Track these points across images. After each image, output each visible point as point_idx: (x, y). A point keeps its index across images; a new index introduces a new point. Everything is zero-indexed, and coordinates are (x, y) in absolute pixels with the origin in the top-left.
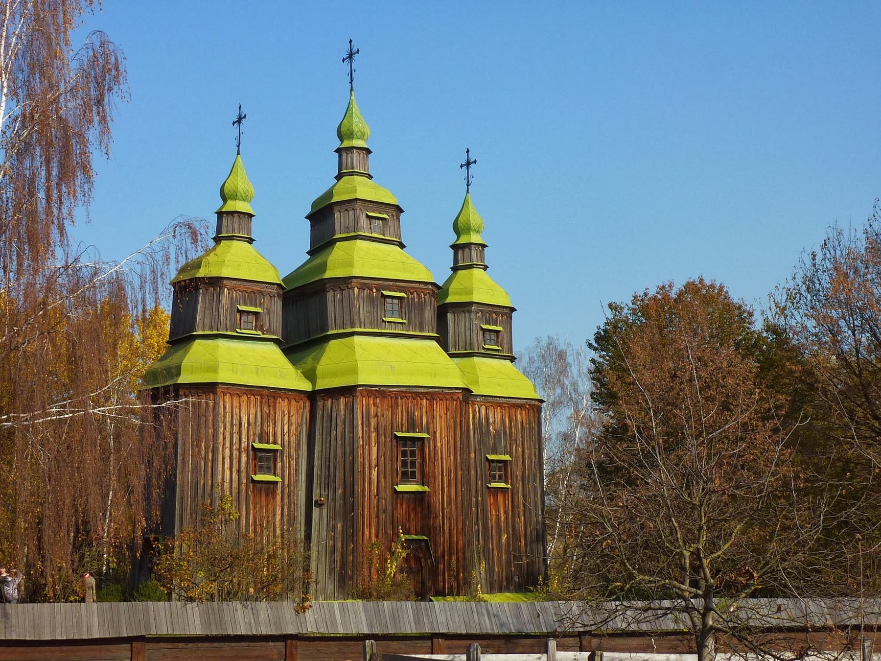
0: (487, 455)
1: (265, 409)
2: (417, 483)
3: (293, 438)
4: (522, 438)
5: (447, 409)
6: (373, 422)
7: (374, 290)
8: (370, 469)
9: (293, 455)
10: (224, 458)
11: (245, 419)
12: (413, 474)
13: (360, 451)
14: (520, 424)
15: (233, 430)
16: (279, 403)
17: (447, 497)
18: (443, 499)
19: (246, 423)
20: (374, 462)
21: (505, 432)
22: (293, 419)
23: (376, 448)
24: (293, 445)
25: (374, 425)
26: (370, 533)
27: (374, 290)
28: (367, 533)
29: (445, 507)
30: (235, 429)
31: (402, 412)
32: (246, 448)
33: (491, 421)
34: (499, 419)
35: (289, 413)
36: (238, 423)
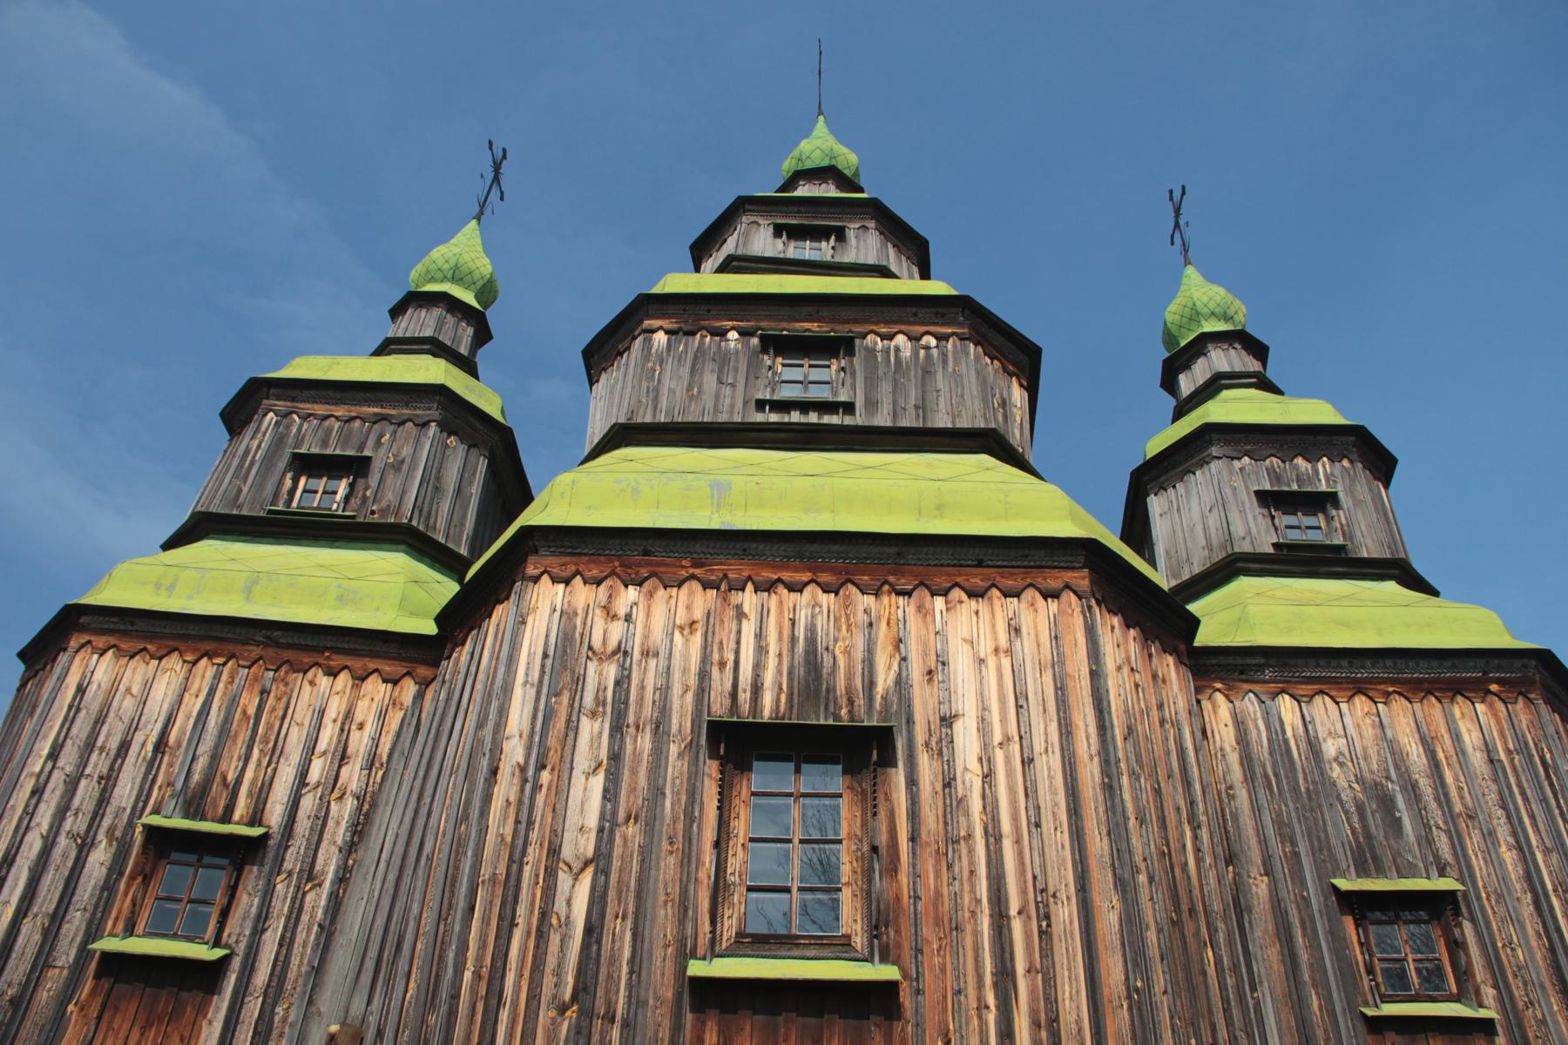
0: (1335, 881)
1: (250, 702)
2: (841, 947)
3: (343, 811)
4: (1504, 807)
5: (1015, 631)
6: (600, 676)
7: (733, 335)
8: (551, 873)
9: (323, 873)
11: (149, 733)
13: (506, 788)
14: (1477, 759)
16: (312, 683)
17: (1036, 1024)
19: (150, 747)
20: (579, 842)
21: (1411, 789)
22: (360, 743)
23: (598, 782)
24: (338, 832)
25: (600, 689)
27: (733, 335)
30: (98, 764)
31: (760, 636)
32: (118, 834)
33: (1330, 748)
34: (1369, 742)
35: (349, 715)
36: (114, 744)
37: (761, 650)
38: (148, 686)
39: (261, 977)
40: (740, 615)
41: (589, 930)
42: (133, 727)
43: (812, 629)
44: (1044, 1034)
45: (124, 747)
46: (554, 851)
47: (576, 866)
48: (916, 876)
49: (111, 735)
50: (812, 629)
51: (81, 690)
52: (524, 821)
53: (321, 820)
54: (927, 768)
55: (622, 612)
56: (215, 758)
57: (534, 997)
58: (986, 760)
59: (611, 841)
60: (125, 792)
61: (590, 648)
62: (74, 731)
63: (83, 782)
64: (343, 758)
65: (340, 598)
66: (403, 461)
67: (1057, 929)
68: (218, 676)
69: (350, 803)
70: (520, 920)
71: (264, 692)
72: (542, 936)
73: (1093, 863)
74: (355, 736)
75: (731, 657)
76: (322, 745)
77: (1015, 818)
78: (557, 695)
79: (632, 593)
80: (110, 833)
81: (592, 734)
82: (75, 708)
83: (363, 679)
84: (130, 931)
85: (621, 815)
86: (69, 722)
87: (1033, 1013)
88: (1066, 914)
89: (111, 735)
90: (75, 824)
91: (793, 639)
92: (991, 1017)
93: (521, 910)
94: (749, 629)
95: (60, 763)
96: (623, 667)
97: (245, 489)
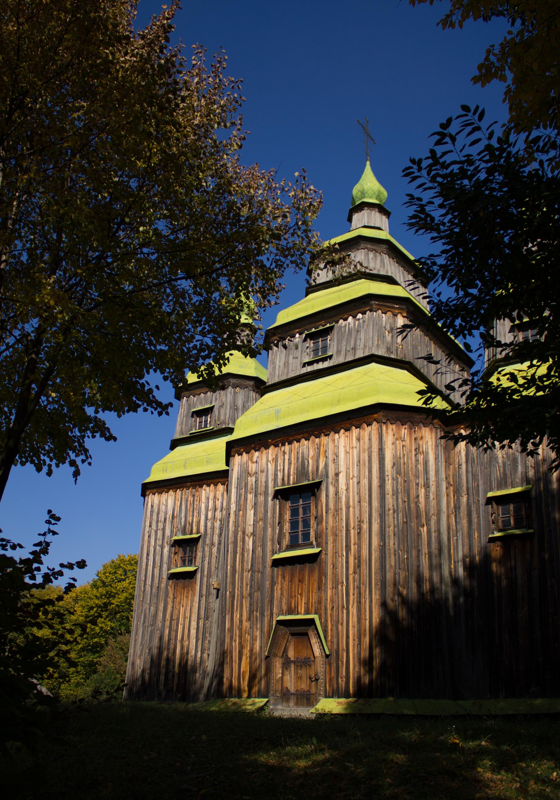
1: (190, 499)
2: (311, 545)
3: (217, 524)
10: (148, 555)
12: (306, 536)
15: (157, 526)
17: (355, 558)
18: (347, 562)
20: (250, 529)
23: (252, 512)
24: (217, 531)
26: (241, 615)
28: (237, 616)
29: (351, 570)
30: (161, 525)
31: (289, 459)
35: (215, 497)
36: (163, 519)
37: (290, 464)
38: (167, 501)
39: (206, 573)
40: (284, 453)
41: (253, 551)
42: (166, 513)
43: (303, 453)
44: (356, 561)
45: (165, 519)
46: (244, 533)
47: (249, 535)
48: (327, 523)
49: (162, 516)
50: (303, 453)
51: (152, 506)
52: (236, 525)
53: (213, 528)
54: (332, 490)
55: (255, 460)
56: (186, 517)
57: (242, 569)
58: (348, 485)
59: (257, 527)
60: (168, 532)
61: (248, 473)
62: (153, 518)
63: (159, 531)
64: (215, 510)
65: (207, 462)
66: (223, 404)
67: (363, 531)
68: (182, 494)
69: (218, 522)
70: (238, 551)
71: (194, 496)
72: (243, 555)
73: (374, 511)
74: (217, 502)
75: (282, 468)
76: (210, 508)
77: (354, 501)
78: (242, 489)
79: (257, 454)
80: (167, 543)
81: (250, 497)
82: (152, 512)
83: (216, 485)
84: (177, 567)
85: (258, 520)
86: (151, 515)
87: (355, 555)
88: (365, 526)
89: (162, 516)
90: (159, 542)
91: (298, 459)
92: (344, 558)
93: (238, 549)
94: (287, 457)
95: (153, 527)
96: (256, 477)
97: (183, 427)
